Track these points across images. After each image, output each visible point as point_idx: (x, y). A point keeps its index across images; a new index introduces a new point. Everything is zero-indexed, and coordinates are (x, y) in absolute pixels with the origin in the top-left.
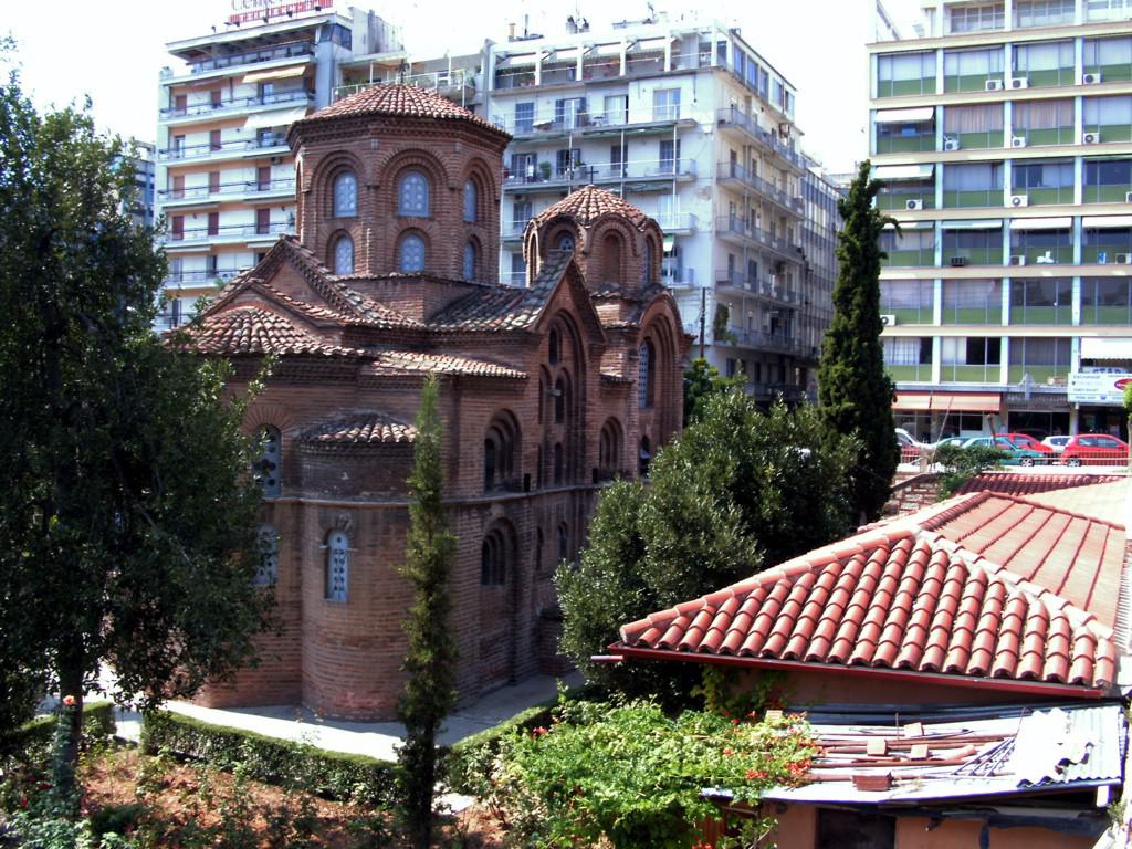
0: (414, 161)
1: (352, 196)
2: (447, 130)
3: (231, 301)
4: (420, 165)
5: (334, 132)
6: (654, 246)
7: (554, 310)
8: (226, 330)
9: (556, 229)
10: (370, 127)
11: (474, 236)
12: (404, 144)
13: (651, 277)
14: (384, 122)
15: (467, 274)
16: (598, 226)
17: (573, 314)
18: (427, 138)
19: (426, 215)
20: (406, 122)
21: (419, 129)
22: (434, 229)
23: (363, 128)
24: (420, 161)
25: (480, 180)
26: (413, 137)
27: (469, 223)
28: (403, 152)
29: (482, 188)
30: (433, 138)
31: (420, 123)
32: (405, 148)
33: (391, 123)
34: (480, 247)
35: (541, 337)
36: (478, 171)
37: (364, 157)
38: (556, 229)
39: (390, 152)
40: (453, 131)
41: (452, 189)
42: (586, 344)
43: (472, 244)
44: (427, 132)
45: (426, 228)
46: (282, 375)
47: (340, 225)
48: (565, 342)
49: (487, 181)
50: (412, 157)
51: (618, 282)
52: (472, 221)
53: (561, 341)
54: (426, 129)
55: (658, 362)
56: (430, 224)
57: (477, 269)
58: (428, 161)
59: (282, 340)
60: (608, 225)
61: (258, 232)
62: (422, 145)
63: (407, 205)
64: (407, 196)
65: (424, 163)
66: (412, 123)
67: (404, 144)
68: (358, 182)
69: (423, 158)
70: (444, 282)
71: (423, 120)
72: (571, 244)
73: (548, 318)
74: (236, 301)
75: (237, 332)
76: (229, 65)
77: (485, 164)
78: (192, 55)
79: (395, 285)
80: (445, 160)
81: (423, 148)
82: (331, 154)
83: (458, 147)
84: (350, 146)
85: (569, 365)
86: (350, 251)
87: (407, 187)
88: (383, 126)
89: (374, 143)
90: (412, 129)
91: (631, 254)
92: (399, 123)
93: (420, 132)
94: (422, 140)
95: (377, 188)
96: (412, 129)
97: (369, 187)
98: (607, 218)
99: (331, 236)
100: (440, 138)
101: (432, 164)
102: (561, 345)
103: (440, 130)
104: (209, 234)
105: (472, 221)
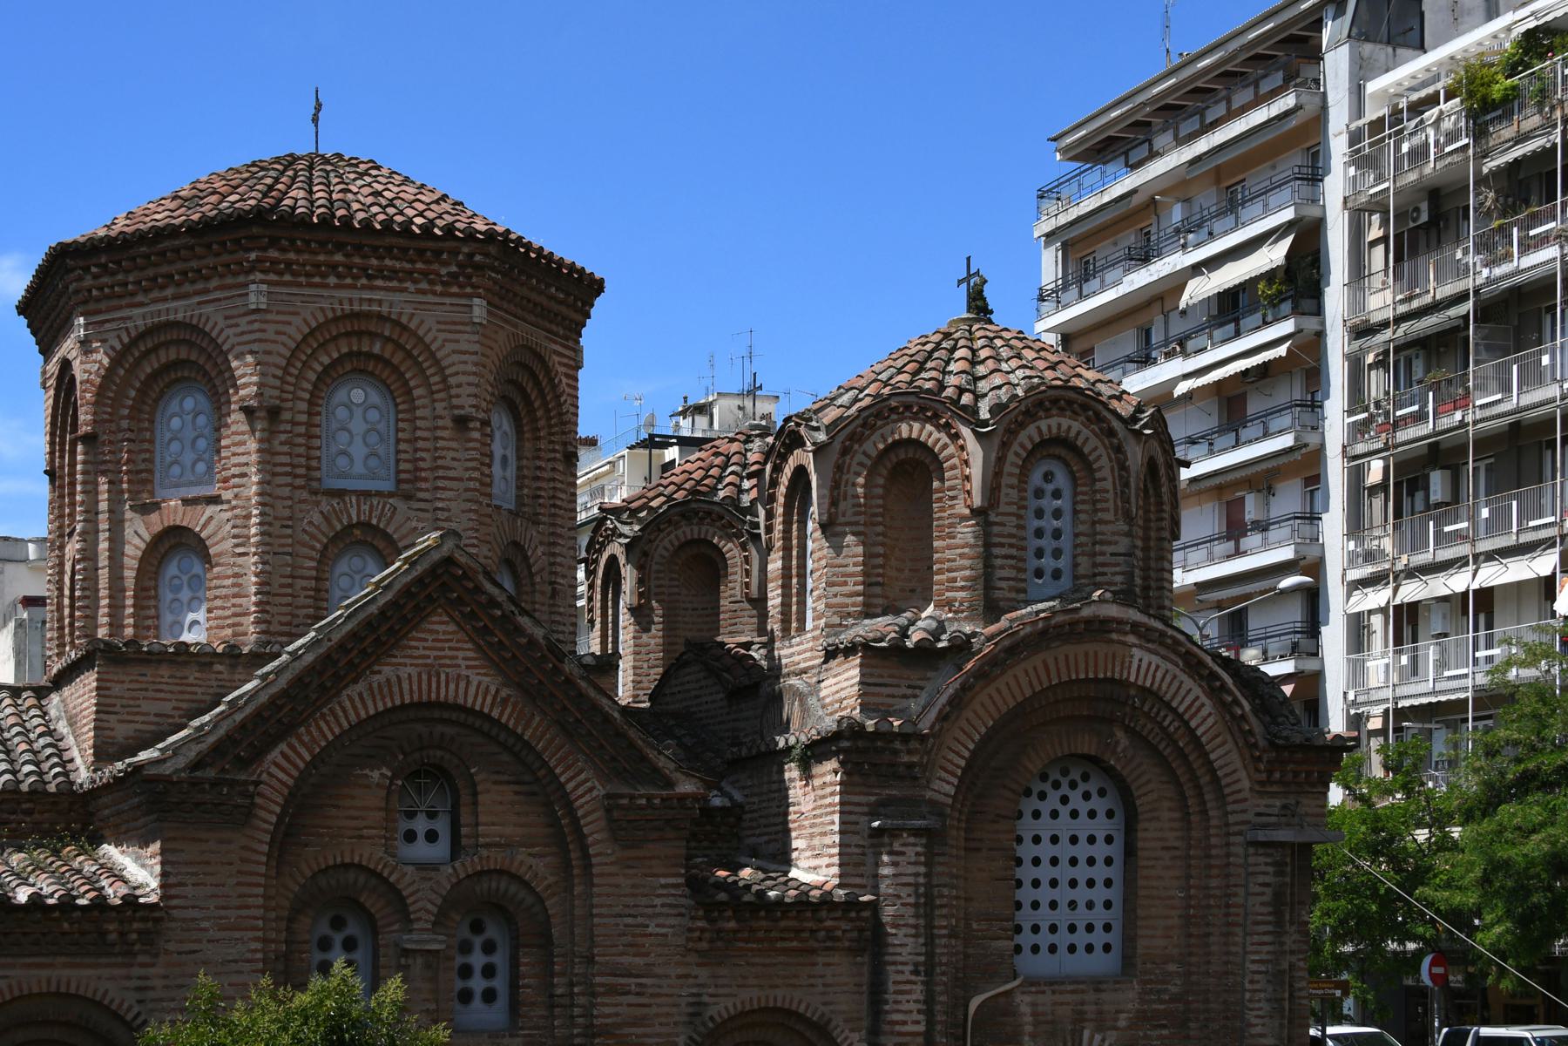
2: (226, 258)
12: (139, 317)
18: (187, 288)
21: (165, 269)
26: (155, 294)
27: (340, 494)
28: (142, 336)
30: (200, 286)
31: (163, 254)
44: (185, 273)
50: (167, 344)
52: (387, 486)
55: (1159, 829)
58: (202, 350)
62: (179, 310)
66: (147, 256)
67: (139, 317)
77: (397, 323)
81: (180, 316)
87: (176, 423)
90: (150, 272)
92: (118, 263)
94: (176, 298)
96: (150, 272)
100: (214, 283)
103: (211, 261)
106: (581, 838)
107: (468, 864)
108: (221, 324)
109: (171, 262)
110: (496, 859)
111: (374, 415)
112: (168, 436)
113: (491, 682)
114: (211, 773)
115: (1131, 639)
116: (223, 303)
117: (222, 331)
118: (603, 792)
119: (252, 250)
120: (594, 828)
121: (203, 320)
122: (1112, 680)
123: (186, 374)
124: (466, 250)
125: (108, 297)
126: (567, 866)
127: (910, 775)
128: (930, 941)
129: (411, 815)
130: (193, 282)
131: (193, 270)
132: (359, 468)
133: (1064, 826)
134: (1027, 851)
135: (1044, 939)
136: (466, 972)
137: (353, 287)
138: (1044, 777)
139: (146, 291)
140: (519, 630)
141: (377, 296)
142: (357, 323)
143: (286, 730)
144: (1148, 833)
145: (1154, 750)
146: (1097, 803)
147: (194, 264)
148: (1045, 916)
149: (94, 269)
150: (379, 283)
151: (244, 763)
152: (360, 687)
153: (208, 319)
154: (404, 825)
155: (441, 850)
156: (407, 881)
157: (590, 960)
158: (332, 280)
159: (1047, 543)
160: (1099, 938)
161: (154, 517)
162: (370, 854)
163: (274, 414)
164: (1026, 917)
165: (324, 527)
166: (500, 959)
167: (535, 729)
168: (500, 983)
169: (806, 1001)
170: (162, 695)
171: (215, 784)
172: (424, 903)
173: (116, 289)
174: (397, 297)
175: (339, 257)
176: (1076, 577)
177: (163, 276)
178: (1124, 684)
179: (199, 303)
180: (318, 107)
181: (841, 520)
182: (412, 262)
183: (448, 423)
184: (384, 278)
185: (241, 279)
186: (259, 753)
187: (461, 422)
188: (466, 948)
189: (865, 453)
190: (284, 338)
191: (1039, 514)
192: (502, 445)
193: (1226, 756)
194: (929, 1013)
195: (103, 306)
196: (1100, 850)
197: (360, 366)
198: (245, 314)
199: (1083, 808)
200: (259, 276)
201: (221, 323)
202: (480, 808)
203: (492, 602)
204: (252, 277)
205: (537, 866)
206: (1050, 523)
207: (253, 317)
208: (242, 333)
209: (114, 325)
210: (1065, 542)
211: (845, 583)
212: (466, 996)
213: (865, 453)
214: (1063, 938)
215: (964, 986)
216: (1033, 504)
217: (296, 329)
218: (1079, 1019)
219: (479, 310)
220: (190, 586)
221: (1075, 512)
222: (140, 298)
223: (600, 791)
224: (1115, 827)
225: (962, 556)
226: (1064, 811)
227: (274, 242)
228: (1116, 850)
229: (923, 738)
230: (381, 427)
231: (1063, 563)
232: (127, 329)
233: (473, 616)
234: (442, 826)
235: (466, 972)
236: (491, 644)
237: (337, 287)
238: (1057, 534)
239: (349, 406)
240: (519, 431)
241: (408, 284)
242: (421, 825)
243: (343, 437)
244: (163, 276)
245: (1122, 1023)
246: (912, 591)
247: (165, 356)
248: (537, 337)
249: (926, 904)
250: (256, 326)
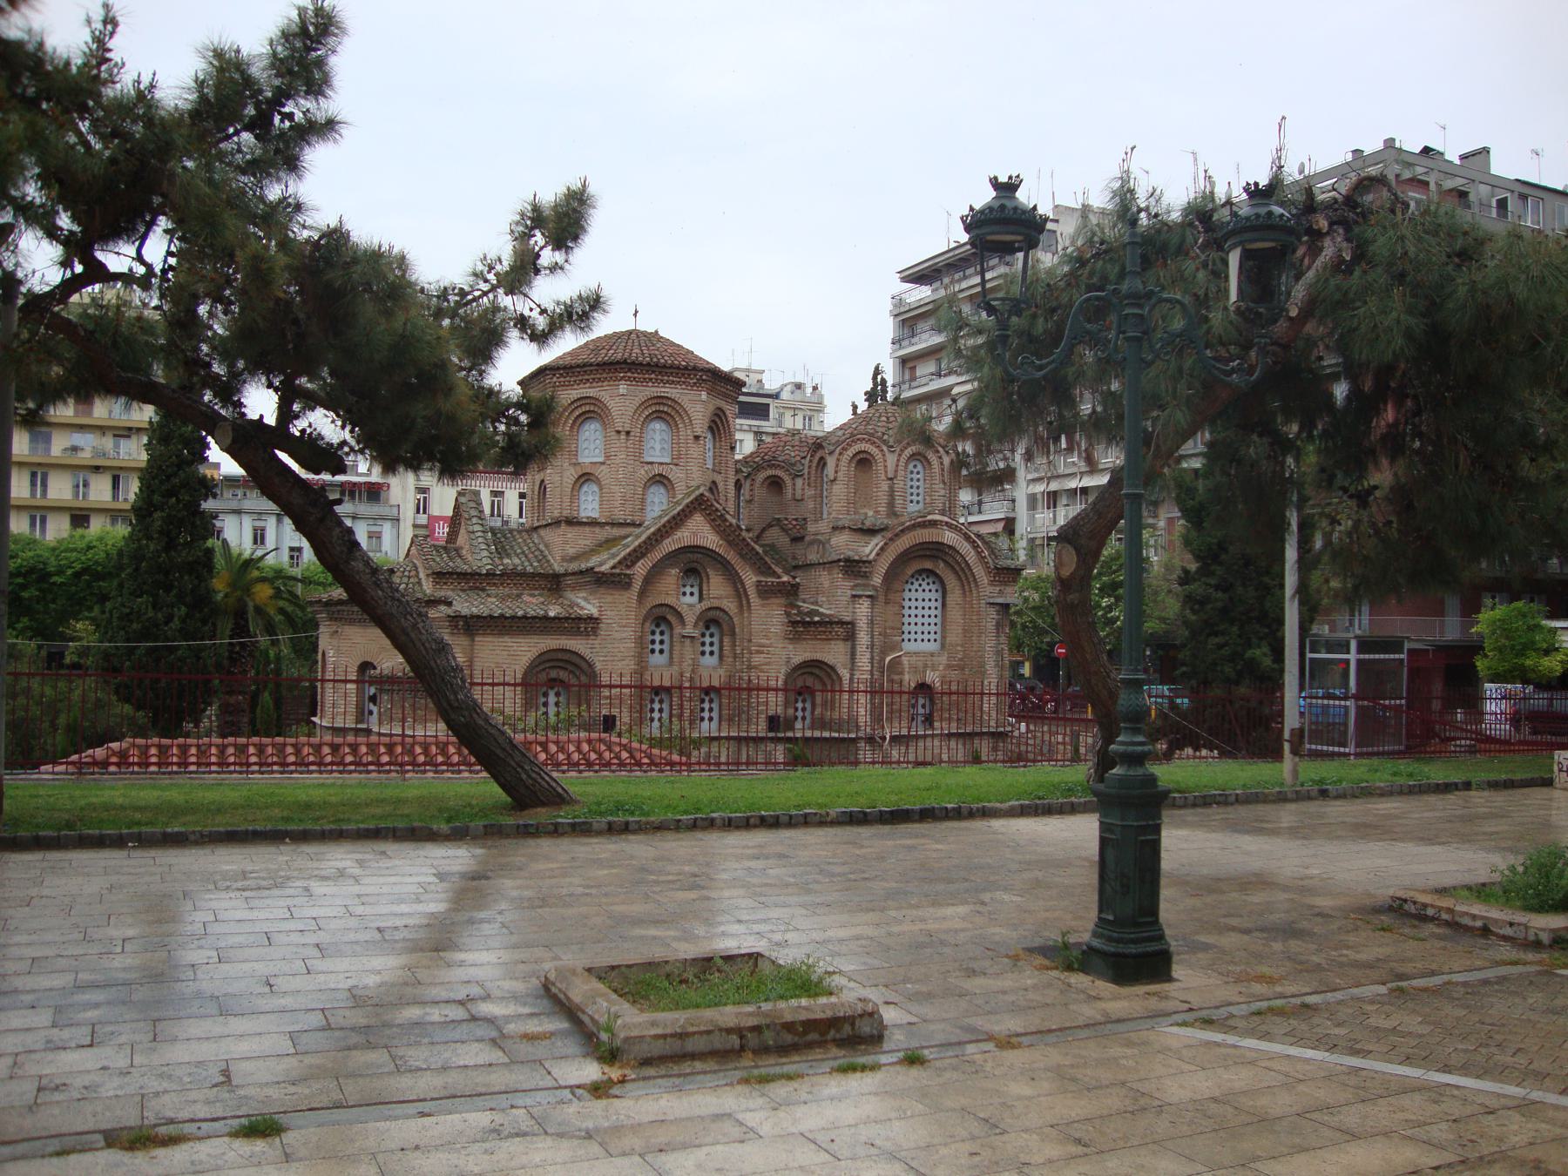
6: (929, 463)
11: (661, 475)
19: (601, 459)
25: (669, 414)
27: (651, 463)
45: (597, 471)
56: (603, 467)
62: (591, 392)
76: (965, 278)
77: (673, 400)
78: (920, 275)
80: (611, 404)
91: (883, 477)
106: (747, 596)
107: (706, 604)
110: (716, 603)
114: (618, 571)
120: (752, 593)
122: (938, 543)
126: (741, 606)
127: (866, 576)
128: (872, 637)
129: (684, 586)
132: (658, 453)
133: (920, 595)
134: (907, 604)
135: (913, 636)
136: (703, 644)
138: (913, 576)
140: (726, 520)
142: (660, 400)
143: (643, 555)
144: (949, 599)
145: (952, 568)
146: (931, 586)
148: (913, 628)
151: (628, 567)
152: (670, 539)
154: (683, 590)
155: (695, 599)
156: (684, 610)
157: (750, 641)
159: (914, 491)
160: (932, 637)
161: (578, 468)
162: (670, 601)
163: (628, 433)
164: (906, 628)
166: (715, 640)
167: (731, 556)
168: (716, 648)
169: (829, 658)
171: (619, 575)
172: (690, 618)
178: (943, 544)
180: (636, 312)
186: (634, 563)
188: (703, 635)
191: (912, 480)
192: (709, 445)
193: (979, 571)
194: (872, 663)
196: (933, 604)
197: (659, 416)
199: (927, 588)
203: (717, 510)
205: (730, 606)
206: (915, 484)
210: (921, 491)
212: (703, 653)
214: (919, 637)
215: (884, 653)
216: (910, 476)
217: (637, 401)
218: (926, 666)
219: (704, 396)
223: (754, 579)
224: (939, 595)
226: (920, 589)
227: (630, 370)
228: (939, 604)
229: (870, 562)
231: (920, 498)
234: (696, 590)
235: (703, 644)
238: (918, 487)
239: (654, 430)
240: (714, 438)
242: (688, 590)
243: (652, 443)
245: (941, 668)
247: (584, 409)
248: (722, 404)
249: (871, 623)
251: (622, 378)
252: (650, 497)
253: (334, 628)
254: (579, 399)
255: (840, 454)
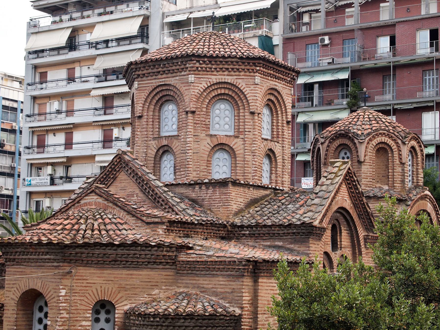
0: (223, 91)
1: (174, 119)
2: (248, 67)
3: (78, 202)
4: (228, 95)
5: (160, 69)
7: (335, 208)
8: (73, 225)
9: (338, 142)
10: (188, 65)
11: (270, 150)
12: (215, 78)
13: (415, 181)
14: (198, 61)
15: (265, 181)
16: (370, 140)
17: (351, 211)
18: (232, 73)
19: (232, 133)
20: (216, 61)
21: (226, 66)
22: (237, 144)
23: (182, 66)
24: (227, 92)
26: (221, 73)
27: (266, 140)
28: (214, 84)
29: (277, 112)
31: (227, 62)
32: (215, 81)
33: (204, 62)
34: (275, 158)
35: (324, 229)
36: (273, 98)
37: (183, 89)
38: (338, 142)
39: (204, 85)
40: (253, 67)
41: (253, 113)
42: (362, 233)
43: (268, 156)
44: (233, 69)
46: (115, 261)
47: (165, 142)
48: (345, 233)
49: (281, 106)
50: (221, 88)
51: (388, 184)
52: (269, 138)
53: (341, 233)
54: (232, 66)
56: (236, 140)
57: (273, 176)
59: (118, 232)
60: (379, 139)
61: (104, 147)
62: (229, 79)
63: (217, 126)
64: (217, 119)
65: (230, 93)
66: (221, 62)
67: (215, 78)
68: (179, 108)
69: (230, 89)
70: (247, 185)
71: (229, 59)
72: (348, 154)
73: (330, 214)
74: (82, 202)
75: (83, 227)
77: (279, 93)
79: (208, 188)
80: (247, 91)
81: (229, 81)
82: (158, 87)
83: (258, 79)
84: (172, 80)
85: (348, 252)
86: (172, 162)
87: (217, 112)
88: (198, 65)
89: (191, 78)
90: (221, 66)
91: (398, 162)
92: (210, 62)
93: (227, 69)
94: (228, 75)
95: (193, 112)
96: (221, 66)
97: (187, 112)
98: (377, 133)
99: (158, 150)
100: (242, 73)
101: (236, 94)
102: (341, 235)
103: (243, 67)
104: (66, 149)
105: (269, 138)
108: (244, 86)
109: (229, 65)
111: (227, 112)
112: (215, 115)
113: (349, 201)
115: (428, 200)
116: (245, 80)
117: (244, 88)
118: (364, 234)
119: (258, 66)
121: (238, 84)
123: (230, 100)
124: (293, 74)
125: (204, 71)
130: (235, 72)
131: (236, 69)
137: (273, 81)
139: (217, 71)
141: (277, 84)
147: (237, 67)
149: (201, 62)
150: (277, 80)
153: (239, 84)
158: (269, 78)
161: (214, 139)
165: (264, 149)
170: (241, 196)
173: (208, 69)
174: (280, 85)
175: (272, 72)
176: (413, 182)
177: (225, 68)
179: (236, 79)
181: (366, 161)
182: (284, 76)
183: (285, 122)
184: (278, 80)
185: (252, 74)
187: (288, 122)
189: (372, 144)
190: (261, 93)
195: (201, 73)
198: (253, 85)
200: (258, 74)
201: (244, 86)
202: (342, 237)
203: (354, 181)
204: (256, 74)
207: (256, 86)
208: (252, 90)
209: (205, 79)
211: (367, 178)
213: (372, 144)
220: (222, 162)
221: (413, 165)
222: (215, 73)
225: (398, 175)
230: (230, 116)
232: (209, 81)
233: (349, 184)
236: (351, 192)
237: (271, 80)
241: (281, 82)
244: (225, 68)
246: (378, 182)
250: (257, 89)
251: (257, 71)
252: (215, 162)
253: (68, 269)
254: (217, 84)
255: (368, 143)
